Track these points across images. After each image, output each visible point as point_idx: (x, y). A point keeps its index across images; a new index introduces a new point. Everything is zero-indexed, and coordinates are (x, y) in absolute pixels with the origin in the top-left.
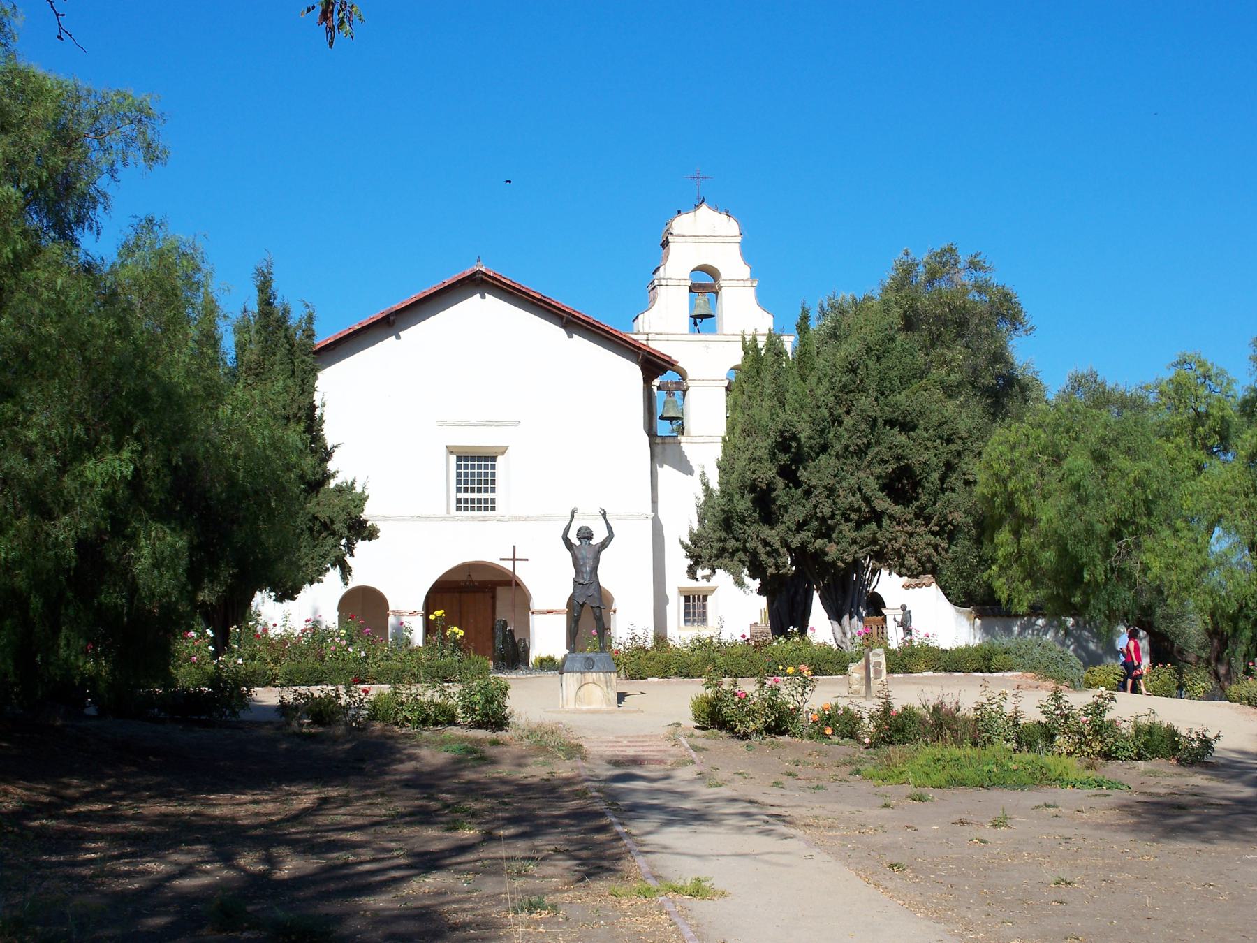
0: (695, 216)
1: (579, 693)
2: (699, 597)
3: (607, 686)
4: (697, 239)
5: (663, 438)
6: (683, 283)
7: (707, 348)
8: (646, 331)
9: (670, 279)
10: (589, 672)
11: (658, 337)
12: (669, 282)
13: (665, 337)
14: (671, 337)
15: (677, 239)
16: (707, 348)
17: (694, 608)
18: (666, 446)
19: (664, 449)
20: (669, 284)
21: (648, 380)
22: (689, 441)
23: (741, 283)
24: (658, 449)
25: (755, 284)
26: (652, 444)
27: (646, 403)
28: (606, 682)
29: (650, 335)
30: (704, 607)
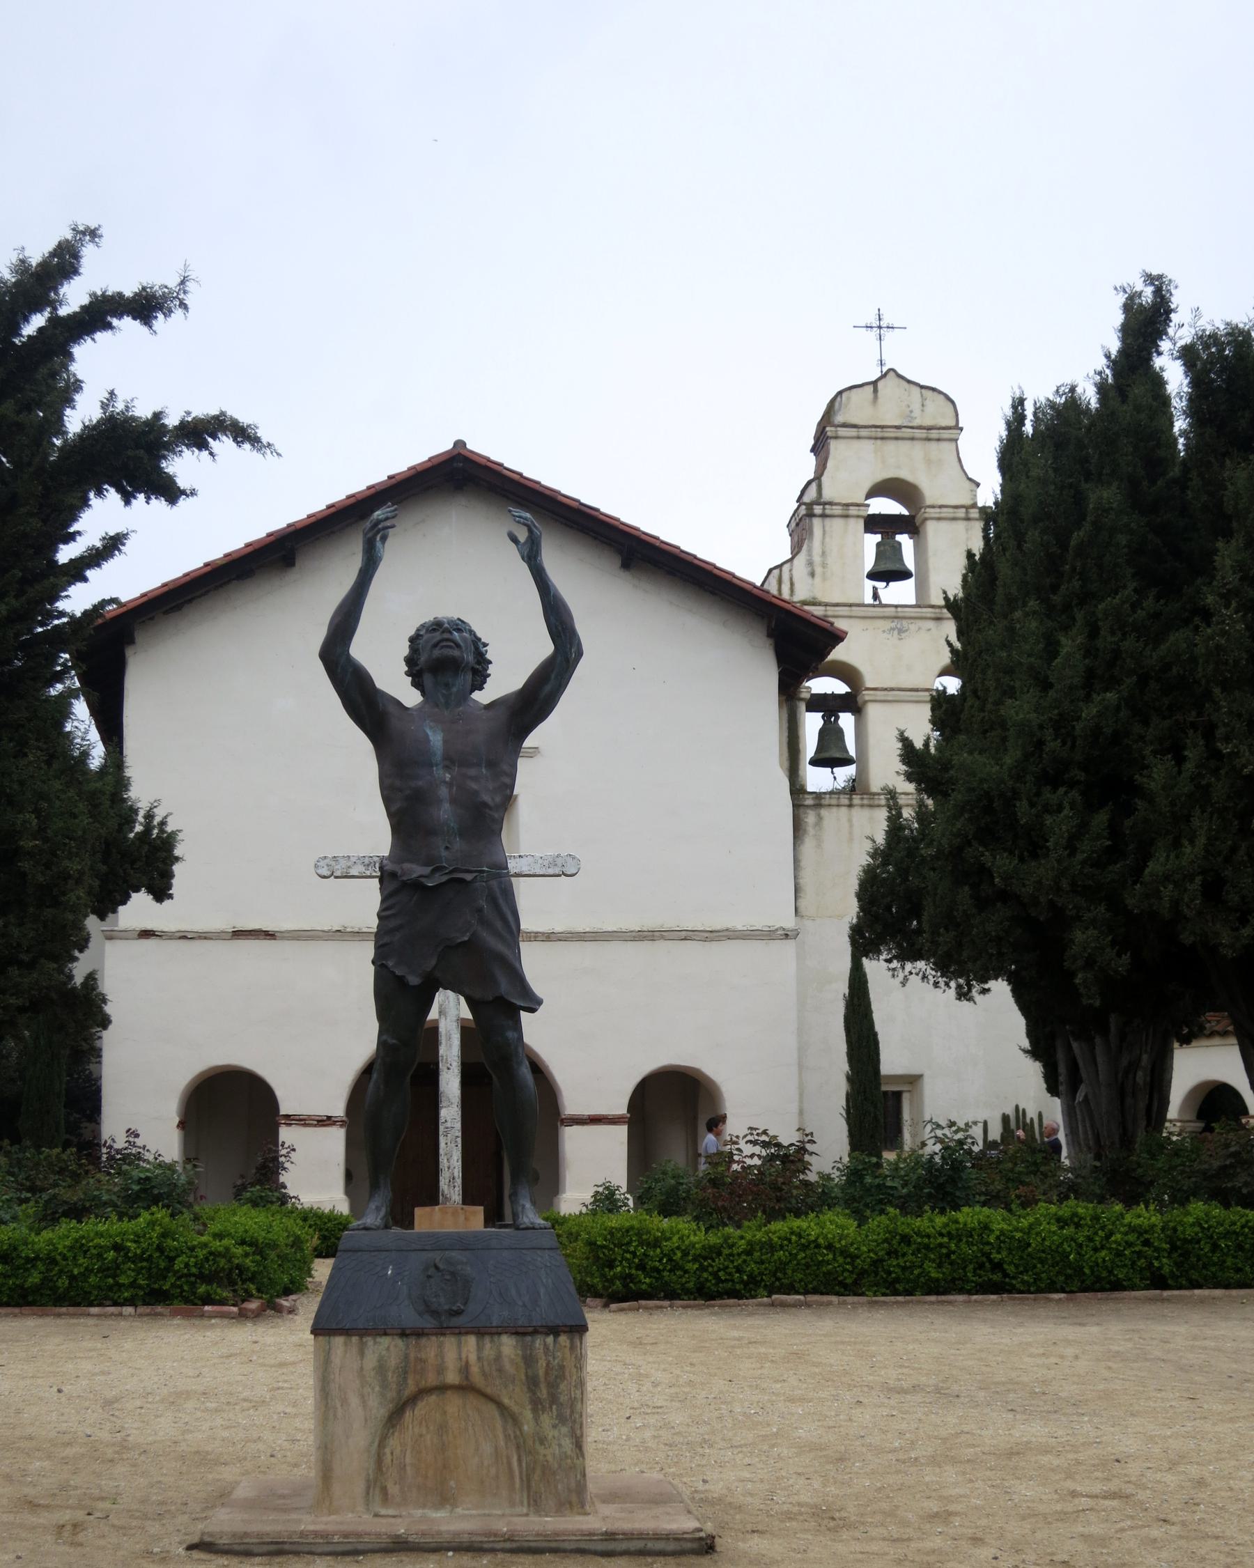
0: (876, 391)
1: (394, 1442)
3: (537, 1404)
4: (879, 433)
5: (818, 796)
7: (900, 631)
9: (831, 503)
10: (441, 1331)
15: (842, 432)
16: (900, 631)
18: (824, 812)
19: (820, 818)
20: (828, 512)
21: (789, 689)
22: (865, 802)
23: (961, 513)
24: (810, 818)
26: (797, 806)
27: (786, 734)
28: (532, 1383)
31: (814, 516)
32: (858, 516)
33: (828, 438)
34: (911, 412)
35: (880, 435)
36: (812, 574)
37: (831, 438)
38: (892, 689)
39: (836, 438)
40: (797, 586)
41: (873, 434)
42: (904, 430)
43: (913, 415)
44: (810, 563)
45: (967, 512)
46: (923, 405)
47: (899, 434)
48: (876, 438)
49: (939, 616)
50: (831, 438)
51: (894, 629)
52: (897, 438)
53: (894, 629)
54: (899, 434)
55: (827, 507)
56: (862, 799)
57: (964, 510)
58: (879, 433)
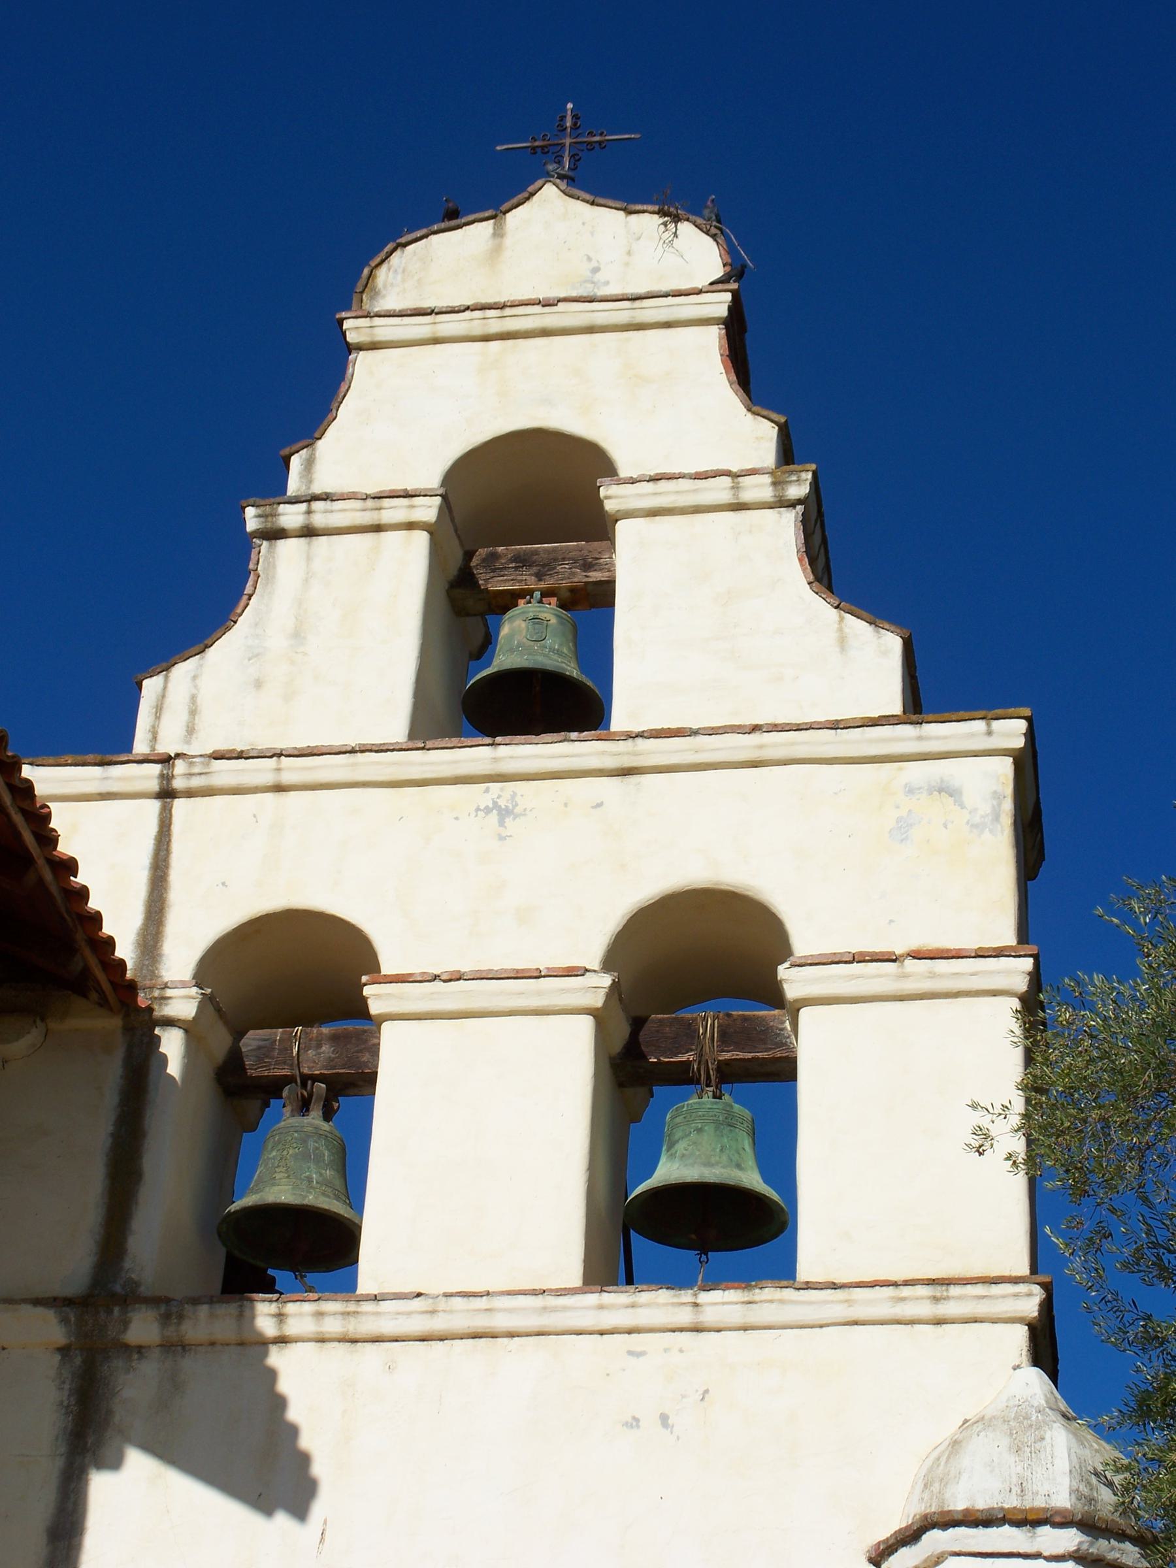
0: (498, 233)
4: (494, 323)
6: (395, 511)
7: (504, 813)
8: (167, 747)
11: (226, 773)
12: (322, 515)
13: (260, 771)
14: (294, 772)
15: (385, 329)
16: (504, 813)
18: (188, 1364)
19: (174, 1384)
22: (333, 1326)
23: (719, 490)
25: (799, 489)
29: (180, 767)
32: (410, 526)
33: (350, 348)
34: (596, 270)
35: (495, 326)
36: (258, 684)
37: (360, 348)
38: (458, 977)
39: (374, 346)
41: (477, 328)
42: (562, 306)
43: (599, 277)
44: (255, 655)
45: (736, 488)
46: (629, 253)
47: (550, 318)
48: (486, 338)
49: (628, 762)
50: (360, 348)
51: (488, 810)
52: (545, 333)
53: (488, 810)
54: (550, 318)
55: (317, 505)
56: (320, 1315)
57: (726, 481)
58: (494, 323)
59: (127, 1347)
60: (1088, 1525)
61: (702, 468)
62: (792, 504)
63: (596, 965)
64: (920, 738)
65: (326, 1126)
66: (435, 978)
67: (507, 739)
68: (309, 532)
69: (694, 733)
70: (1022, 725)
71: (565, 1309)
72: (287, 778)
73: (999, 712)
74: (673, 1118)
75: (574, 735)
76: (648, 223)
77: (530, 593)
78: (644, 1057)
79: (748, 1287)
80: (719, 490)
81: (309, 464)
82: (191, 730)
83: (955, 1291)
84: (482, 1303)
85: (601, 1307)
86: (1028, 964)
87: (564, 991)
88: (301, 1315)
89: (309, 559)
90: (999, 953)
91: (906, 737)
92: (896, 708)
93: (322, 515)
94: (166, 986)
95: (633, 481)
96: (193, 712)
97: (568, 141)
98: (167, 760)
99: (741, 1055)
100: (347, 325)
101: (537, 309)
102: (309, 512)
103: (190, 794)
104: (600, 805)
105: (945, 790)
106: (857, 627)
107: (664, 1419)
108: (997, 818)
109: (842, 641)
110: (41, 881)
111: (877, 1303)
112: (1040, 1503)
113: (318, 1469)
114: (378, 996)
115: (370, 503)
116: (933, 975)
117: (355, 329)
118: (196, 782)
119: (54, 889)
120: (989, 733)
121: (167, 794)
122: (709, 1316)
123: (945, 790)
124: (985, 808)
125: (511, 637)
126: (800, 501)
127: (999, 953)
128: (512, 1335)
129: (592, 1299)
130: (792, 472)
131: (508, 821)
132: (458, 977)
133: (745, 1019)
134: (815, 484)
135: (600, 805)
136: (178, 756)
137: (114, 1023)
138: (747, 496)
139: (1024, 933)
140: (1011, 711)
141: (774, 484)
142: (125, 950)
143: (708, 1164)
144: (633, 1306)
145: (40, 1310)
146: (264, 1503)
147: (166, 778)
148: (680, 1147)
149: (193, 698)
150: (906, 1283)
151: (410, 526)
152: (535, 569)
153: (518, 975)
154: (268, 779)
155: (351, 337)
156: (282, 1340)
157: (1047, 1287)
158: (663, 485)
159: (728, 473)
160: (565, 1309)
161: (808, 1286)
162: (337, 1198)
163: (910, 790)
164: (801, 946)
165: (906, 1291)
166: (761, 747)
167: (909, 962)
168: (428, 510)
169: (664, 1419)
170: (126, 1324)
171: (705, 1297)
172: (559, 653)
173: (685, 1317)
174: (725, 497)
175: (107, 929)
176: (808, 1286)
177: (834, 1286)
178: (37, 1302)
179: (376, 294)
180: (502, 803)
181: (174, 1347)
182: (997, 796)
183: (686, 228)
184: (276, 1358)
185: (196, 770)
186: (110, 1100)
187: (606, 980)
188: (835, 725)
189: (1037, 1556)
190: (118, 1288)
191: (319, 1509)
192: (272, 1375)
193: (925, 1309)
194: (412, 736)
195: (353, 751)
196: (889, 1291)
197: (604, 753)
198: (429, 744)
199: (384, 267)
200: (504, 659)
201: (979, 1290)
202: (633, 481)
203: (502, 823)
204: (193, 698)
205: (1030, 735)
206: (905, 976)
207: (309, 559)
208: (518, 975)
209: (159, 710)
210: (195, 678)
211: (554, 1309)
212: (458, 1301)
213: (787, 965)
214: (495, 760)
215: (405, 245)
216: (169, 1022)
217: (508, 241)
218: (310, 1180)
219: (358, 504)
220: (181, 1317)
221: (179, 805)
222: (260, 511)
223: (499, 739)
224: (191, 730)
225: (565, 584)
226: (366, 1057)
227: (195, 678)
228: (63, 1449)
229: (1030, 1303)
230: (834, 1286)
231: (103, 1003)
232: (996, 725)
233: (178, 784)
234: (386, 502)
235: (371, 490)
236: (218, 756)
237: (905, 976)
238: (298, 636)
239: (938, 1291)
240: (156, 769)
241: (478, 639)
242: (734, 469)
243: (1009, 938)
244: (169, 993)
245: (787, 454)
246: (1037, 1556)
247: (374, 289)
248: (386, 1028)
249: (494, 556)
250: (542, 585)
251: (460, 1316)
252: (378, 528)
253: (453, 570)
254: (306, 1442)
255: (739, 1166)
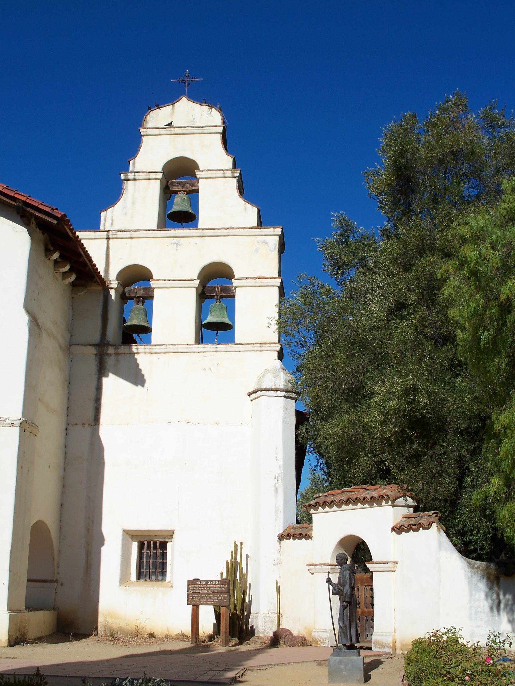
0: (173, 109)
2: (149, 543)
6: (153, 176)
7: (177, 245)
8: (107, 229)
11: (120, 234)
12: (138, 176)
13: (127, 234)
14: (134, 234)
15: (149, 132)
16: (177, 245)
17: (148, 557)
19: (117, 361)
20: (137, 177)
22: (147, 350)
23: (220, 174)
25: (237, 174)
29: (111, 233)
30: (164, 556)
31: (129, 180)
32: (156, 179)
34: (194, 119)
35: (173, 132)
36: (126, 214)
37: (144, 136)
38: (169, 280)
39: (147, 135)
40: (115, 222)
43: (195, 120)
45: (224, 173)
46: (201, 115)
50: (144, 136)
51: (174, 244)
52: (184, 134)
53: (174, 244)
55: (136, 174)
56: (145, 348)
57: (222, 172)
59: (108, 354)
60: (286, 391)
61: (217, 169)
62: (236, 177)
63: (196, 278)
64: (260, 232)
65: (142, 307)
66: (165, 280)
67: (178, 229)
68: (135, 180)
69: (215, 229)
70: (281, 230)
71: (191, 348)
72: (133, 236)
73: (276, 227)
74: (211, 307)
75: (191, 229)
76: (205, 108)
77: (181, 191)
78: (205, 294)
79: (226, 344)
80: (220, 174)
81: (134, 163)
82: (112, 224)
83: (264, 345)
84: (176, 346)
85: (198, 348)
86: (280, 280)
87: (190, 284)
88: (141, 348)
89: (135, 185)
90: (275, 278)
91: (257, 231)
92: (255, 224)
93: (138, 176)
94: (111, 281)
95: (202, 171)
96: (112, 220)
97: (187, 80)
98: (108, 231)
99: (224, 294)
100: (141, 130)
101: (182, 129)
102: (135, 175)
103: (113, 238)
104: (196, 243)
105: (265, 242)
106: (248, 205)
107: (210, 369)
108: (275, 249)
109: (245, 209)
110: (89, 268)
111: (250, 347)
112: (278, 387)
113: (146, 377)
114: (153, 284)
115: (147, 174)
116: (262, 282)
117: (143, 131)
118: (114, 236)
119: (92, 269)
120: (274, 231)
121: (108, 238)
122: (218, 350)
123: (265, 242)
124: (273, 247)
125: (177, 202)
126: (237, 177)
127: (275, 278)
128: (181, 353)
129: (197, 346)
130: (235, 170)
131: (178, 246)
132: (169, 280)
133: (225, 287)
134: (240, 173)
135: (196, 243)
136: (110, 230)
137: (100, 288)
138: (226, 175)
139: (280, 274)
140: (278, 227)
141: (232, 173)
142: (102, 273)
143: (218, 317)
144: (204, 347)
145: (91, 347)
146: (136, 383)
147: (108, 235)
148: (213, 313)
149: (112, 217)
150: (255, 344)
151: (156, 179)
152: (182, 186)
153: (181, 280)
154: (129, 236)
155: (142, 133)
156: (138, 353)
157: (281, 345)
158: (209, 172)
159: (222, 170)
160: (191, 348)
161: (237, 344)
162: (146, 322)
163: (258, 242)
164: (237, 275)
165: (255, 345)
166: (229, 232)
167: (257, 279)
168: (160, 176)
169: (210, 369)
170: (108, 350)
171: (218, 346)
172: (187, 206)
173: (214, 350)
174: (222, 175)
175: (99, 270)
176: (237, 344)
177: (242, 344)
178: (90, 345)
179: (147, 122)
180: (177, 242)
181: (117, 354)
182: (275, 244)
183: (213, 110)
184: (136, 356)
185: (114, 234)
186: (101, 304)
187: (198, 281)
188: (244, 228)
189: (277, 396)
190: (105, 342)
191: (146, 385)
192: (136, 359)
193: (259, 349)
194: (158, 228)
195: (146, 231)
196: (252, 345)
197: (197, 233)
198: (162, 230)
199: (149, 115)
200: (176, 208)
201: (269, 345)
202: (202, 171)
203: (177, 247)
204: (112, 217)
205: (282, 231)
206: (256, 282)
207: (135, 185)
208: (181, 280)
209: (105, 219)
210: (112, 212)
211: (190, 348)
212: (171, 346)
213: (233, 279)
214: (175, 233)
215: (153, 111)
216: (112, 288)
217: (175, 111)
218: (140, 319)
219: (145, 174)
220: (118, 349)
221: (110, 240)
222: (124, 175)
223: (176, 229)
224: (112, 224)
225: (188, 189)
226: (150, 293)
227: (112, 212)
228: (97, 373)
229: (278, 348)
230: (242, 344)
231: (99, 284)
232: (275, 229)
233: (110, 237)
234: (151, 174)
235: (148, 171)
236: (118, 231)
237: (256, 282)
238: (133, 203)
239: (261, 345)
240: (106, 233)
241: (169, 198)
242: (224, 169)
243: (276, 275)
244: (111, 282)
245: (235, 166)
246: (277, 396)
247: (146, 121)
248: (155, 290)
249: (173, 182)
250: (183, 189)
251: (172, 349)
252: (149, 179)
253: (164, 186)
254: (143, 372)
255: (224, 318)
